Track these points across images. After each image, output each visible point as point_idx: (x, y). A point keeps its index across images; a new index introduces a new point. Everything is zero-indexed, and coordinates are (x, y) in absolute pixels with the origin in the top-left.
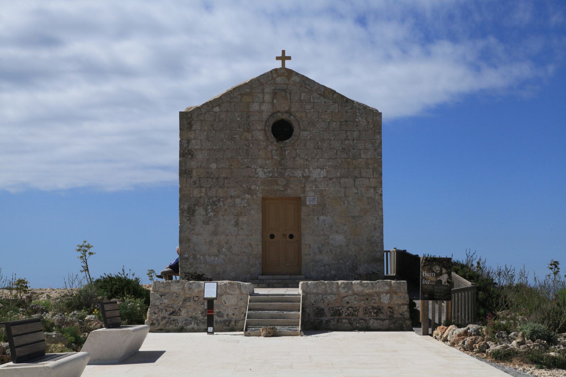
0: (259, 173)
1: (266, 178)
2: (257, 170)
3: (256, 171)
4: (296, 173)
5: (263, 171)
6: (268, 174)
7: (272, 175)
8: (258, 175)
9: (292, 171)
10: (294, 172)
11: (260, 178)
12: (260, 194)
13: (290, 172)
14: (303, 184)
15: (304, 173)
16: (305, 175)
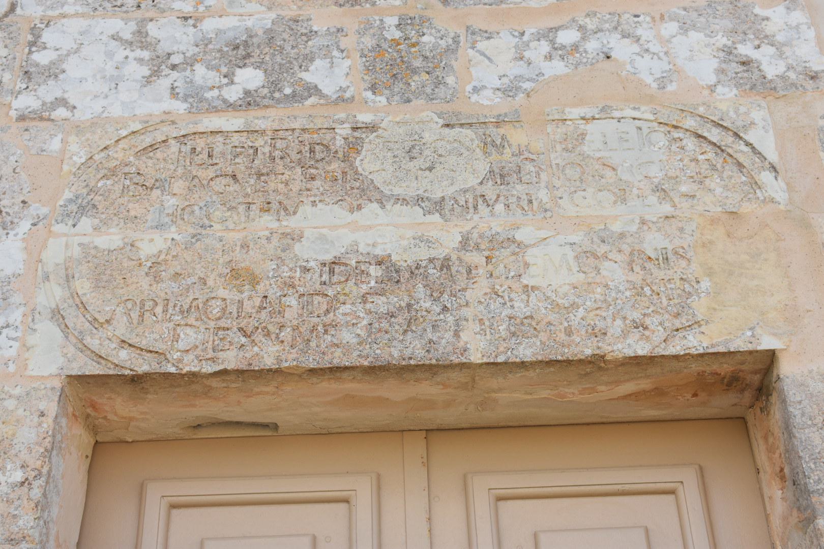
0: (73, 68)
1: (169, 119)
2: (47, 36)
3: (35, 43)
4: (622, 49)
5: (141, 39)
6: (200, 69)
7: (275, 86)
8: (49, 91)
9: (567, 37)
10: (592, 46)
11: (79, 129)
12: (48, 330)
13: (544, 47)
14: (766, 177)
15: (745, 50)
16: (772, 69)
